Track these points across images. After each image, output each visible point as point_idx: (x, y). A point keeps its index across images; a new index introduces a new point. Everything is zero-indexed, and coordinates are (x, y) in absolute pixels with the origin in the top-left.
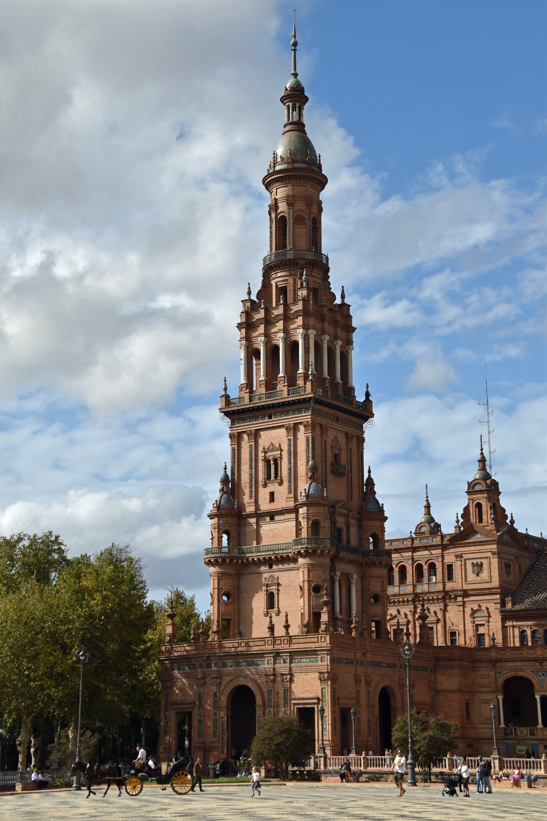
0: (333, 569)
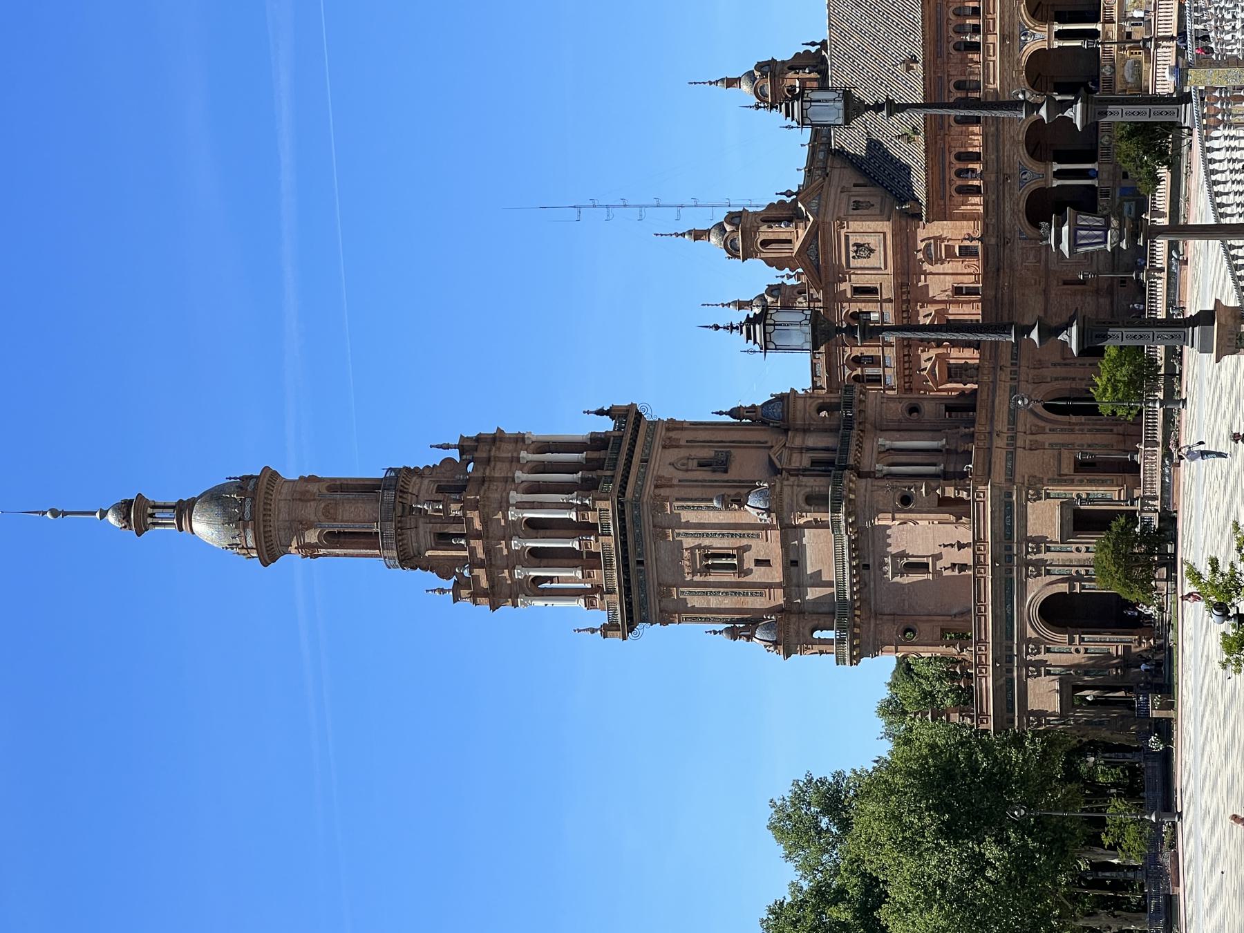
0: (870, 475)
